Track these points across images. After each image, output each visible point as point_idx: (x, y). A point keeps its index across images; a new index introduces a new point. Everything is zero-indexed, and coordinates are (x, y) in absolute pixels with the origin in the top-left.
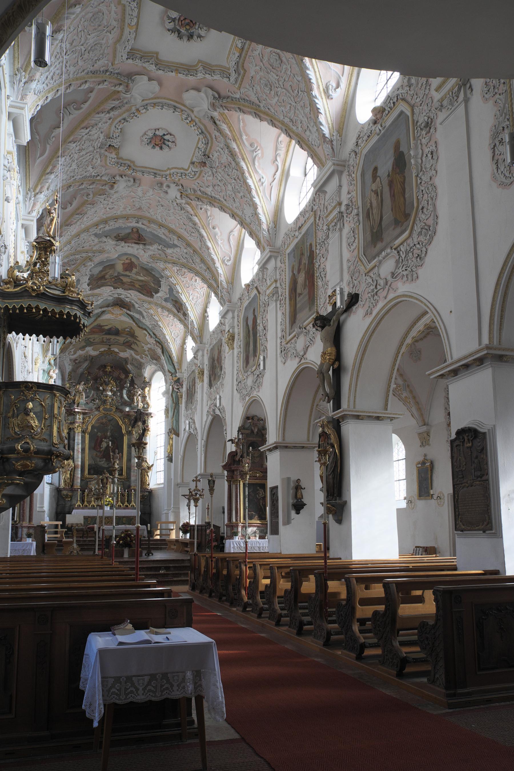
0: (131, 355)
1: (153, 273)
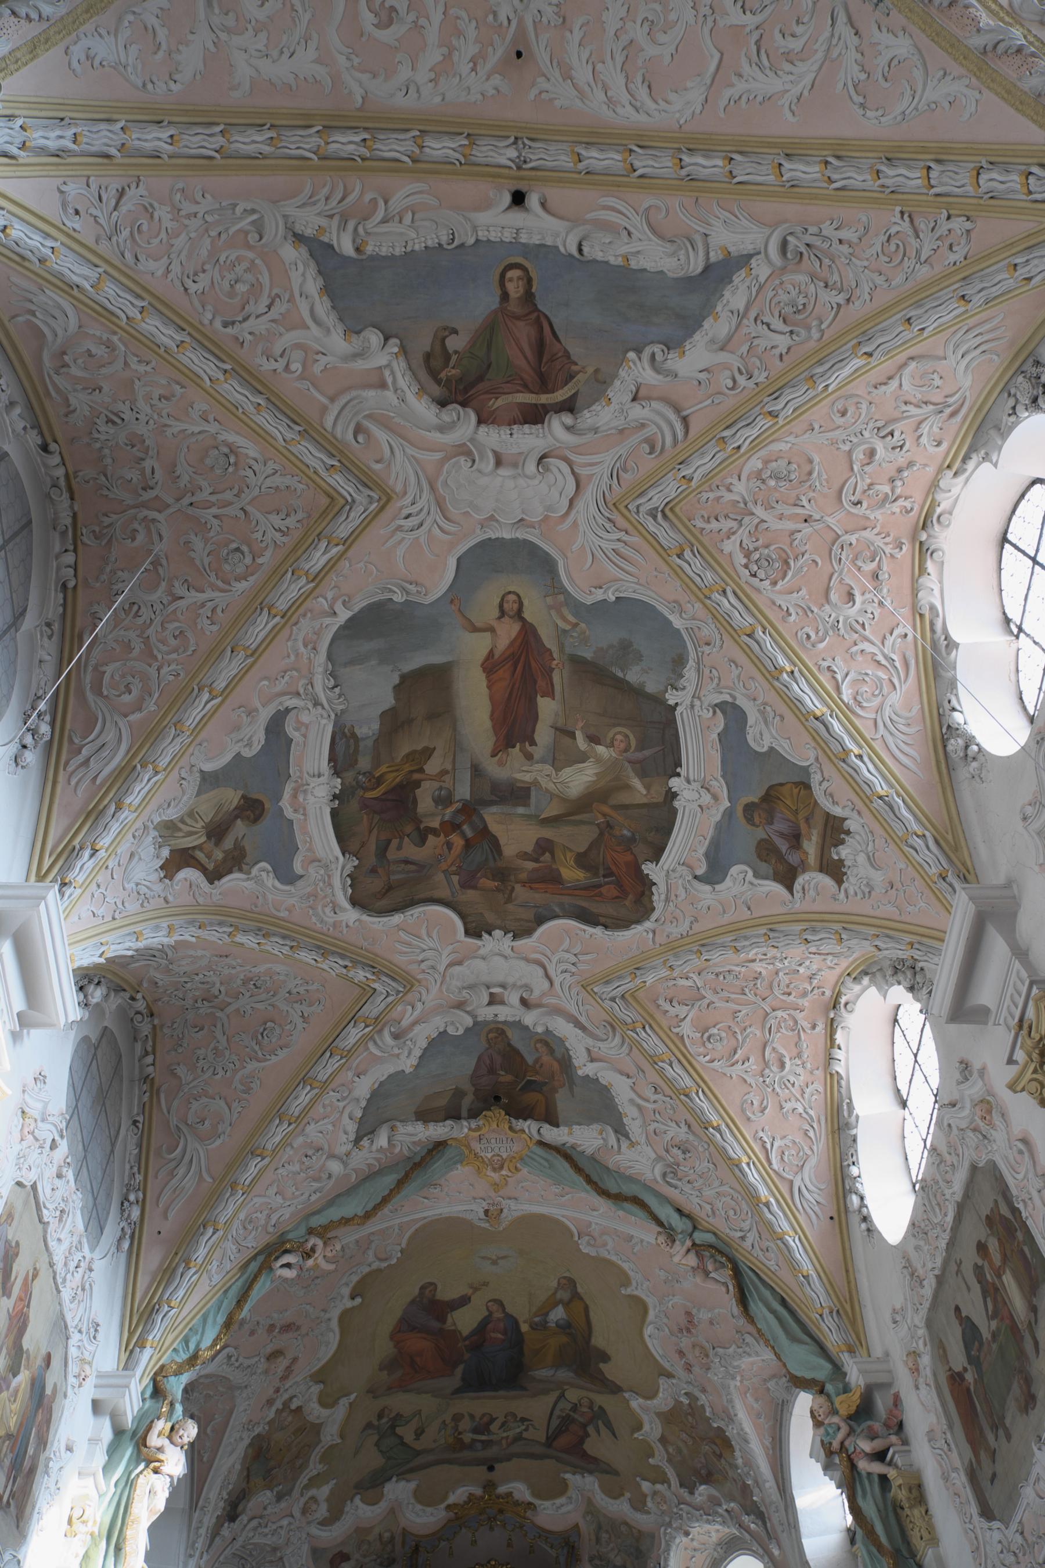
0: (591, 1510)
1: (633, 676)
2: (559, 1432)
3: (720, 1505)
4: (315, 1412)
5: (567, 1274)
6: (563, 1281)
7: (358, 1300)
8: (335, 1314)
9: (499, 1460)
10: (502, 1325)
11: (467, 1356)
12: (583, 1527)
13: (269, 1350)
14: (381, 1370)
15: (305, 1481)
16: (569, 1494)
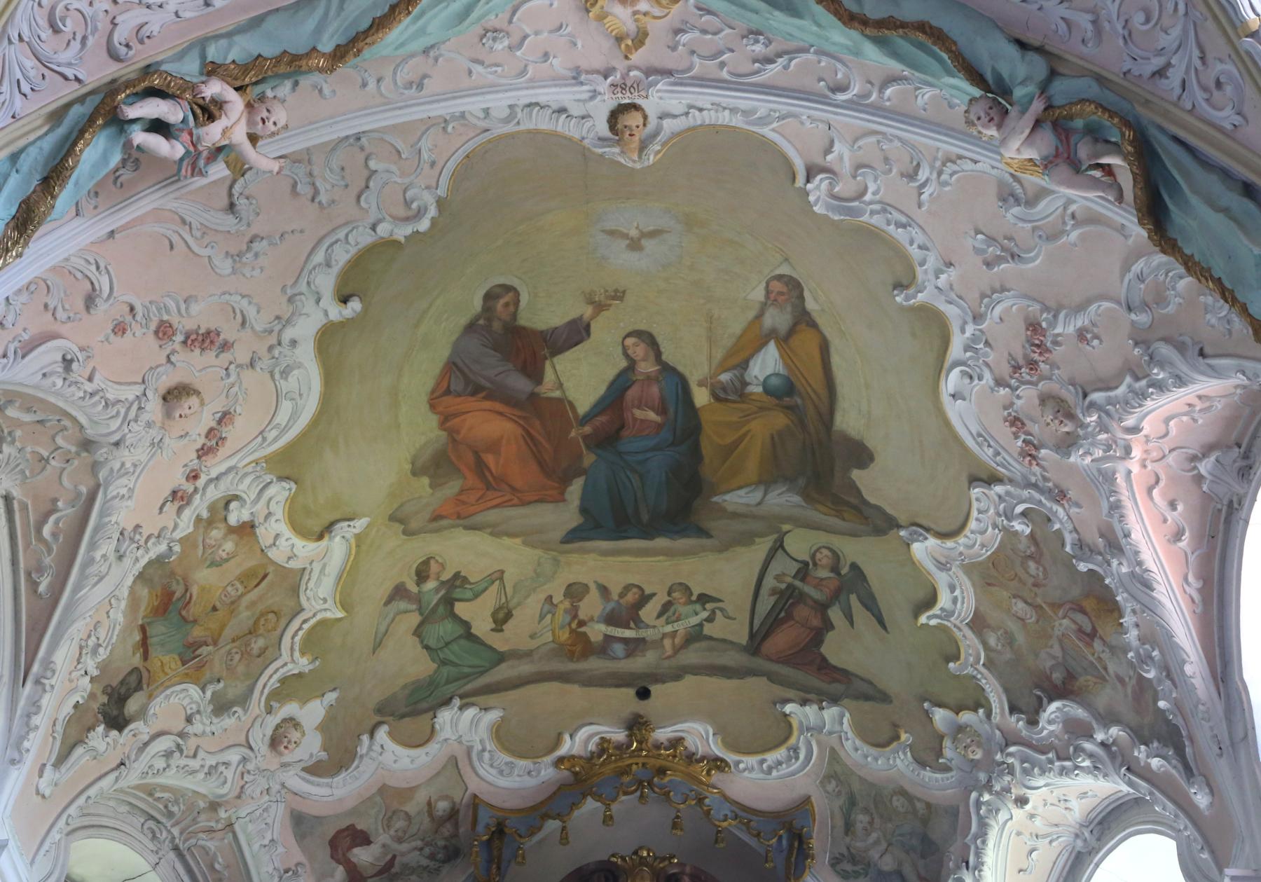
0: (836, 773)
2: (774, 622)
3: (1090, 736)
4: (285, 544)
5: (784, 270)
6: (777, 286)
7: (355, 305)
8: (306, 328)
9: (659, 679)
10: (655, 390)
11: (589, 459)
12: (820, 803)
13: (167, 379)
14: (415, 473)
15: (273, 683)
16: (792, 741)
